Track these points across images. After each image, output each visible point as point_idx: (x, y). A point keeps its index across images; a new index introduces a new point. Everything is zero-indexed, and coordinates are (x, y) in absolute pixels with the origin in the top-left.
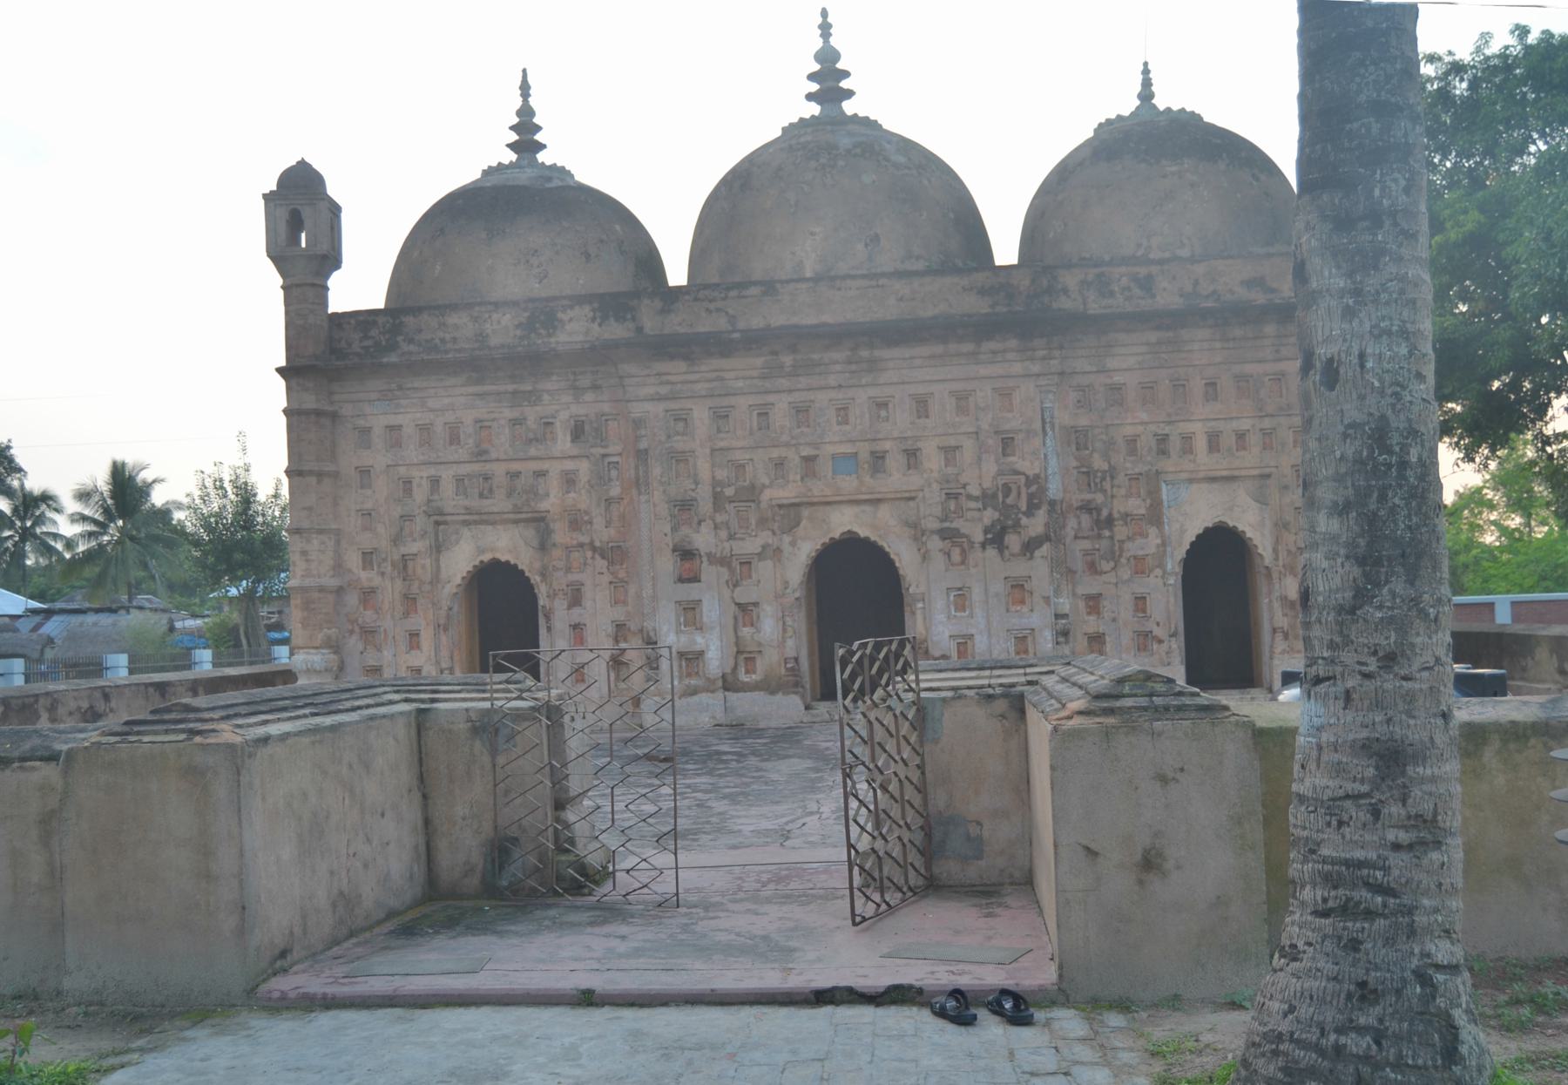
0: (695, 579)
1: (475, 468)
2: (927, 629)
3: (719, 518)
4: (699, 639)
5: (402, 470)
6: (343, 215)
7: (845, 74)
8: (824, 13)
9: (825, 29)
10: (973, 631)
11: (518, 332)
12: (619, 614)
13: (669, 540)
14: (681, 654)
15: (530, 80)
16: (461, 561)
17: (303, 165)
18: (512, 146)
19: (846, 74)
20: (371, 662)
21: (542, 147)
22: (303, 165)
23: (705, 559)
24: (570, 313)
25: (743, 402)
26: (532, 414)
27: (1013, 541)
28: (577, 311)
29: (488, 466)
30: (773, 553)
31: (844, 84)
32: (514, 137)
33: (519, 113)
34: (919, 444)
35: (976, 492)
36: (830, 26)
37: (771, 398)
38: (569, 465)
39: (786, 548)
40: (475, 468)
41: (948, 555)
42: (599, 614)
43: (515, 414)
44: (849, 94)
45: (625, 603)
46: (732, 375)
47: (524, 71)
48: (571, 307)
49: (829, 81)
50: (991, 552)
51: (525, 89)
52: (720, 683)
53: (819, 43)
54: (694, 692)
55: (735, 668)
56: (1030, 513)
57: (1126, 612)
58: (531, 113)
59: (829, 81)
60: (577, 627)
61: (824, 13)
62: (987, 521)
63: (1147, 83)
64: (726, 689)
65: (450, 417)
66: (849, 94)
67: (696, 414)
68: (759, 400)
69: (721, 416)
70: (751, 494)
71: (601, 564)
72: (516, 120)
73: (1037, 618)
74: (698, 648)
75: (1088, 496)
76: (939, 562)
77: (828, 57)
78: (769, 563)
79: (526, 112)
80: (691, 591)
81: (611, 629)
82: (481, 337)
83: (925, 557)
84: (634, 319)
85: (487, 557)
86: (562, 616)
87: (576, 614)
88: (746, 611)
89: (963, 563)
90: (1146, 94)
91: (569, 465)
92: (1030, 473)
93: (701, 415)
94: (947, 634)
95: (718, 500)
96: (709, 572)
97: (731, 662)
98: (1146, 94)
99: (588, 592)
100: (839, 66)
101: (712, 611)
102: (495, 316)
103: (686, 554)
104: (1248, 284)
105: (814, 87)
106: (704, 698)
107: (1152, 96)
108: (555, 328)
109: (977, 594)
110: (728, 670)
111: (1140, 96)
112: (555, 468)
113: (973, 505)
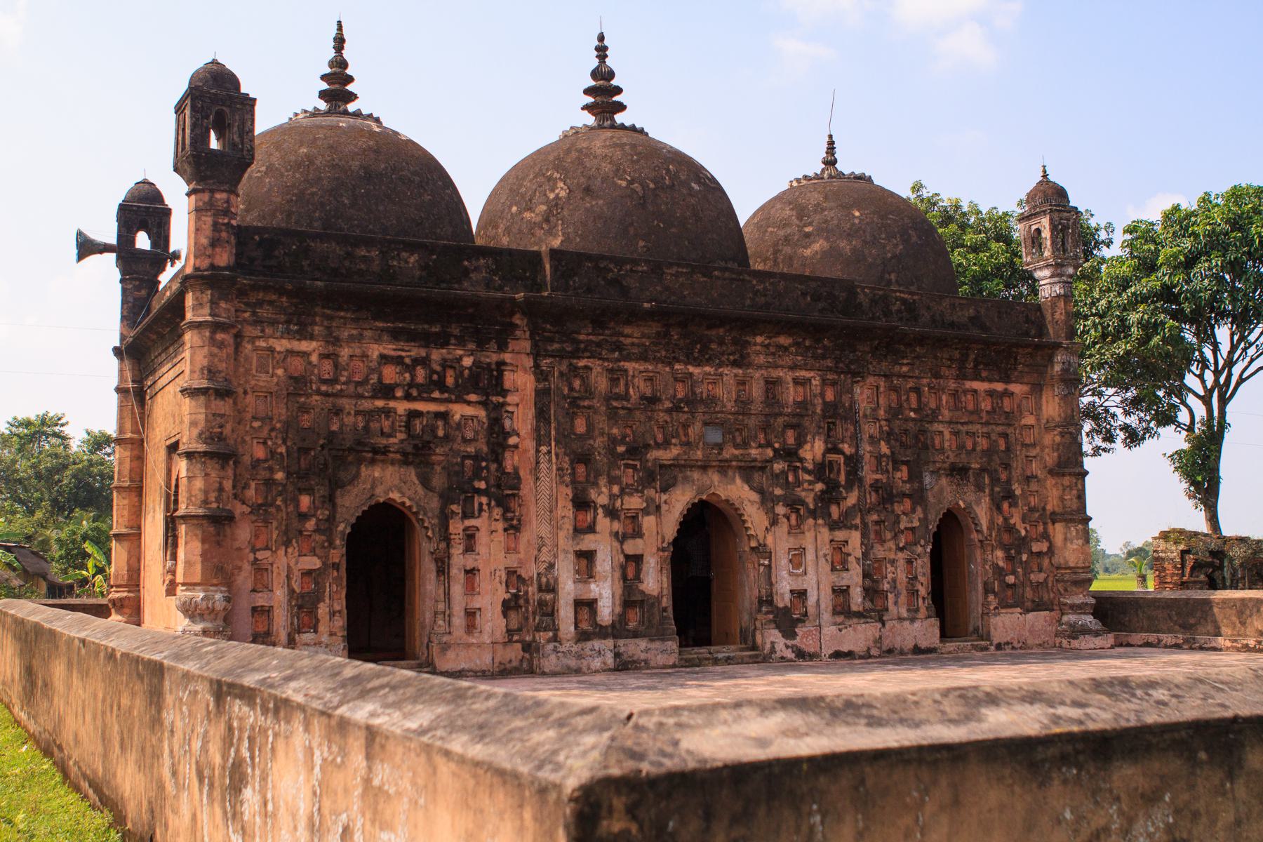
0: (591, 529)
1: (380, 403)
7: (619, 90)
8: (601, 38)
9: (602, 51)
10: (805, 587)
12: (512, 561)
13: (569, 491)
17: (214, 62)
18: (323, 95)
19: (619, 90)
20: (261, 600)
21: (352, 97)
22: (214, 62)
23: (600, 511)
26: (436, 355)
27: (835, 511)
29: (392, 404)
30: (655, 509)
31: (616, 98)
32: (325, 86)
33: (332, 64)
35: (810, 466)
36: (606, 48)
38: (469, 411)
39: (664, 507)
40: (380, 403)
41: (788, 519)
43: (423, 353)
44: (621, 107)
45: (516, 551)
46: (629, 341)
47: (339, 23)
49: (604, 95)
51: (340, 42)
52: (610, 630)
53: (596, 63)
54: (583, 636)
58: (344, 64)
59: (604, 95)
60: (471, 572)
61: (601, 38)
64: (615, 637)
66: (621, 107)
69: (615, 376)
70: (636, 451)
72: (328, 70)
73: (853, 578)
74: (592, 596)
75: (878, 476)
76: (783, 528)
77: (603, 74)
79: (340, 63)
80: (588, 543)
83: (774, 522)
86: (459, 560)
90: (830, 162)
91: (469, 411)
92: (848, 453)
94: (788, 588)
96: (603, 523)
98: (830, 162)
99: (482, 538)
100: (614, 82)
101: (605, 562)
102: (404, 254)
103: (581, 503)
105: (590, 100)
106: (597, 644)
107: (835, 161)
109: (810, 556)
111: (825, 162)
113: (807, 477)
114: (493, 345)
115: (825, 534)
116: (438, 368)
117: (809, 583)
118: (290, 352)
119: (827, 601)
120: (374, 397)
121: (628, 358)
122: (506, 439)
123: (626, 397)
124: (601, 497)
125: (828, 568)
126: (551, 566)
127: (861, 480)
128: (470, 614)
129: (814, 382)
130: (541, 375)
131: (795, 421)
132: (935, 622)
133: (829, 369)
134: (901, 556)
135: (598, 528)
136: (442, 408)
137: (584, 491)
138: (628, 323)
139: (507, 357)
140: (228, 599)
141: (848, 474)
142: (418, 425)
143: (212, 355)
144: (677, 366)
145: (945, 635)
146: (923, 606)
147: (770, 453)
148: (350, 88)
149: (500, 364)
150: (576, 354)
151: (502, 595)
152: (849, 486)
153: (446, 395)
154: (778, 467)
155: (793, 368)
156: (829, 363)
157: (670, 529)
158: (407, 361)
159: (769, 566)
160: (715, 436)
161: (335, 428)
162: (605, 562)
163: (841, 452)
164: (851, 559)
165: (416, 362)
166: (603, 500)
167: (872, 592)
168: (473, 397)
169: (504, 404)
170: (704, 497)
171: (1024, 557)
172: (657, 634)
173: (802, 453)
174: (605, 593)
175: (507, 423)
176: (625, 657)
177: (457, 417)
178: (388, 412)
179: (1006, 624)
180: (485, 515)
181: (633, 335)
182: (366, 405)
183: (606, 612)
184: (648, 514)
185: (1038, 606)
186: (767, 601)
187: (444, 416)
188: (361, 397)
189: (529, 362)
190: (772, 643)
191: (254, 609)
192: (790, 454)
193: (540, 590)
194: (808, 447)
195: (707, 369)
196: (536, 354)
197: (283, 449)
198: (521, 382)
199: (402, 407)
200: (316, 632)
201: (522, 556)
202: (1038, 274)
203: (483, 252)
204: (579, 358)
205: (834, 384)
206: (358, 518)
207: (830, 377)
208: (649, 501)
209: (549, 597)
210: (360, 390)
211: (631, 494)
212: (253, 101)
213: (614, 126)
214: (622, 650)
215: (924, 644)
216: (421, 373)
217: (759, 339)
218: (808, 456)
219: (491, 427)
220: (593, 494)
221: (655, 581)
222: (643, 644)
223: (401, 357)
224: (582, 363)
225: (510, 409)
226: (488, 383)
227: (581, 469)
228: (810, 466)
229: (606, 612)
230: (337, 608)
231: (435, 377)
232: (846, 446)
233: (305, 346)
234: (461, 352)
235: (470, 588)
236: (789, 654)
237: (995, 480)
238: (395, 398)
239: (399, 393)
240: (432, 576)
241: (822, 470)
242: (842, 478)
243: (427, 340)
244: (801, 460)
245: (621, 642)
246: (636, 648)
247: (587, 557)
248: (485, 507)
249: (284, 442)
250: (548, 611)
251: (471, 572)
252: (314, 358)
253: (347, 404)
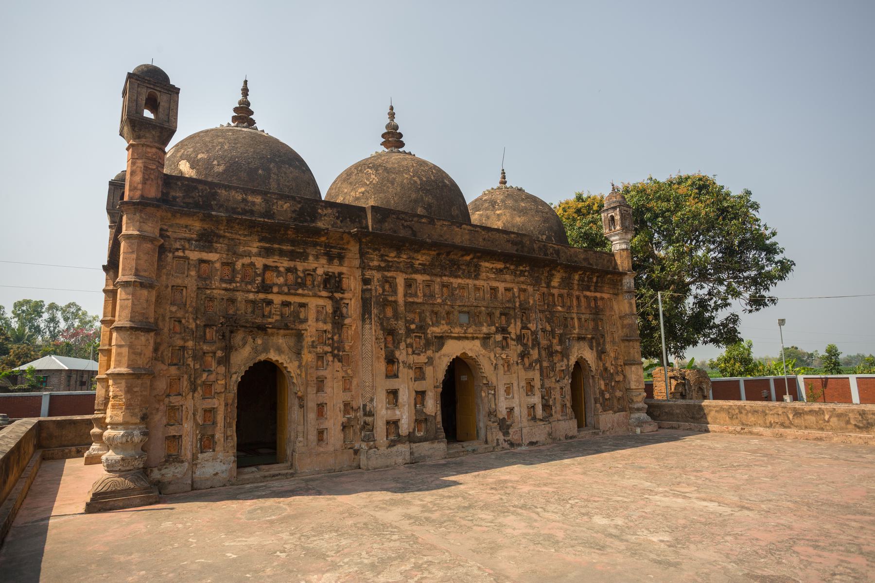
0: (396, 376)
1: (262, 296)
2: (496, 405)
3: (409, 341)
4: (398, 412)
5: (208, 292)
8: (392, 108)
9: (392, 115)
11: (294, 215)
12: (347, 397)
13: (383, 352)
14: (388, 423)
15: (249, 87)
16: (243, 357)
20: (172, 431)
24: (325, 212)
25: (419, 278)
26: (300, 266)
28: (329, 211)
29: (270, 297)
30: (430, 361)
34: (494, 311)
37: (434, 278)
42: (334, 396)
45: (349, 390)
46: (418, 262)
47: (246, 82)
48: (326, 208)
49: (393, 138)
50: (520, 366)
51: (245, 91)
53: (388, 121)
54: (392, 444)
55: (414, 430)
56: (533, 348)
57: (558, 396)
58: (249, 104)
59: (393, 138)
61: (392, 108)
62: (519, 352)
63: (504, 177)
64: (410, 442)
65: (247, 260)
67: (397, 280)
68: (427, 278)
69: (409, 284)
70: (422, 328)
71: (338, 365)
73: (536, 399)
74: (397, 418)
76: (501, 370)
78: (431, 368)
80: (393, 384)
81: (342, 406)
82: (268, 214)
84: (360, 222)
85: (262, 357)
87: (322, 398)
88: (421, 395)
89: (509, 370)
91: (321, 302)
93: (400, 280)
95: (409, 331)
96: (403, 372)
97: (413, 425)
99: (328, 383)
101: (405, 396)
102: (280, 202)
103: (391, 360)
104: (585, 259)
106: (400, 447)
108: (316, 218)
109: (515, 387)
110: (411, 430)
112: (313, 303)
114: (336, 261)
115: (523, 374)
116: (301, 275)
117: (515, 403)
118: (202, 261)
119: (525, 412)
120: (257, 292)
121: (416, 271)
122: (343, 320)
123: (416, 295)
124: (401, 355)
126: (372, 400)
127: (539, 344)
128: (321, 433)
130: (366, 281)
132: (575, 421)
133: (523, 283)
134: (558, 386)
135: (400, 375)
137: (392, 352)
138: (418, 251)
139: (344, 269)
140: (145, 434)
141: (533, 340)
142: (287, 311)
143: (138, 259)
144: (444, 278)
145: (580, 426)
146: (569, 410)
147: (493, 328)
149: (340, 274)
150: (388, 268)
151: (341, 419)
153: (306, 292)
154: (499, 337)
155: (505, 281)
156: (522, 279)
157: (441, 376)
158: (282, 269)
159: (494, 395)
161: (231, 312)
162: (405, 396)
163: (528, 329)
164: (536, 388)
165: (288, 270)
167: (546, 407)
168: (324, 294)
169: (342, 299)
171: (613, 384)
172: (434, 439)
174: (405, 417)
175: (344, 310)
176: (416, 455)
178: (270, 303)
179: (607, 419)
180: (330, 368)
181: (421, 258)
182: (251, 296)
183: (405, 427)
185: (620, 410)
186: (492, 414)
188: (249, 291)
189: (358, 273)
190: (498, 440)
191: (167, 438)
192: (503, 330)
193: (365, 415)
194: (512, 325)
195: (460, 281)
196: (363, 267)
197: (193, 326)
198: (353, 284)
200: (214, 451)
201: (353, 393)
202: (612, 239)
203: (329, 204)
204: (388, 271)
206: (250, 367)
207: (524, 287)
209: (369, 419)
210: (250, 287)
211: (419, 354)
212: (177, 91)
213: (399, 152)
214: (415, 450)
215: (570, 434)
216: (291, 277)
217: (487, 264)
218: (513, 331)
219: (335, 312)
220: (397, 354)
221: (432, 406)
222: (426, 445)
223: (277, 267)
224: (389, 274)
225: (346, 301)
226: (333, 284)
227: (390, 338)
228: (514, 337)
229: (405, 427)
230: (229, 433)
231: (299, 280)
233: (213, 256)
234: (316, 265)
236: (506, 445)
237: (598, 344)
238: (272, 292)
239: (275, 289)
240: (296, 408)
241: (519, 339)
242: (530, 344)
243: (293, 256)
244: (510, 333)
245: (414, 445)
246: (424, 448)
247: (394, 394)
248: (330, 363)
249: (195, 320)
250: (368, 428)
252: (218, 265)
253: (240, 296)
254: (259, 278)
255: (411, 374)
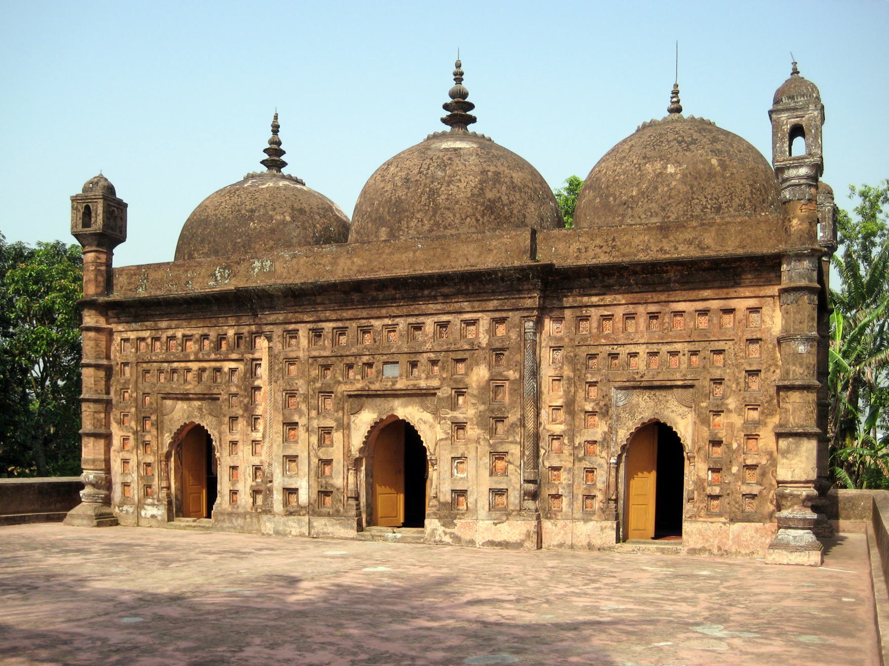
1: (183, 365)
6: (128, 209)
12: (256, 461)
29: (190, 365)
30: (345, 427)
35: (475, 392)
38: (233, 365)
43: (206, 331)
68: (340, 324)
91: (233, 365)
122: (253, 382)
125: (487, 473)
129: (481, 322)
131: (460, 356)
136: (218, 364)
142: (205, 375)
148: (283, 158)
152: (512, 405)
160: (391, 371)
166: (302, 421)
170: (384, 417)
173: (467, 380)
177: (226, 370)
178: (189, 370)
184: (337, 430)
187: (218, 370)
199: (195, 366)
205: (502, 320)
207: (497, 315)
208: (336, 420)
216: (206, 342)
224: (291, 327)
228: (475, 392)
232: (511, 372)
235: (233, 478)
251: (234, 468)
254: (180, 348)
255: (314, 439)
